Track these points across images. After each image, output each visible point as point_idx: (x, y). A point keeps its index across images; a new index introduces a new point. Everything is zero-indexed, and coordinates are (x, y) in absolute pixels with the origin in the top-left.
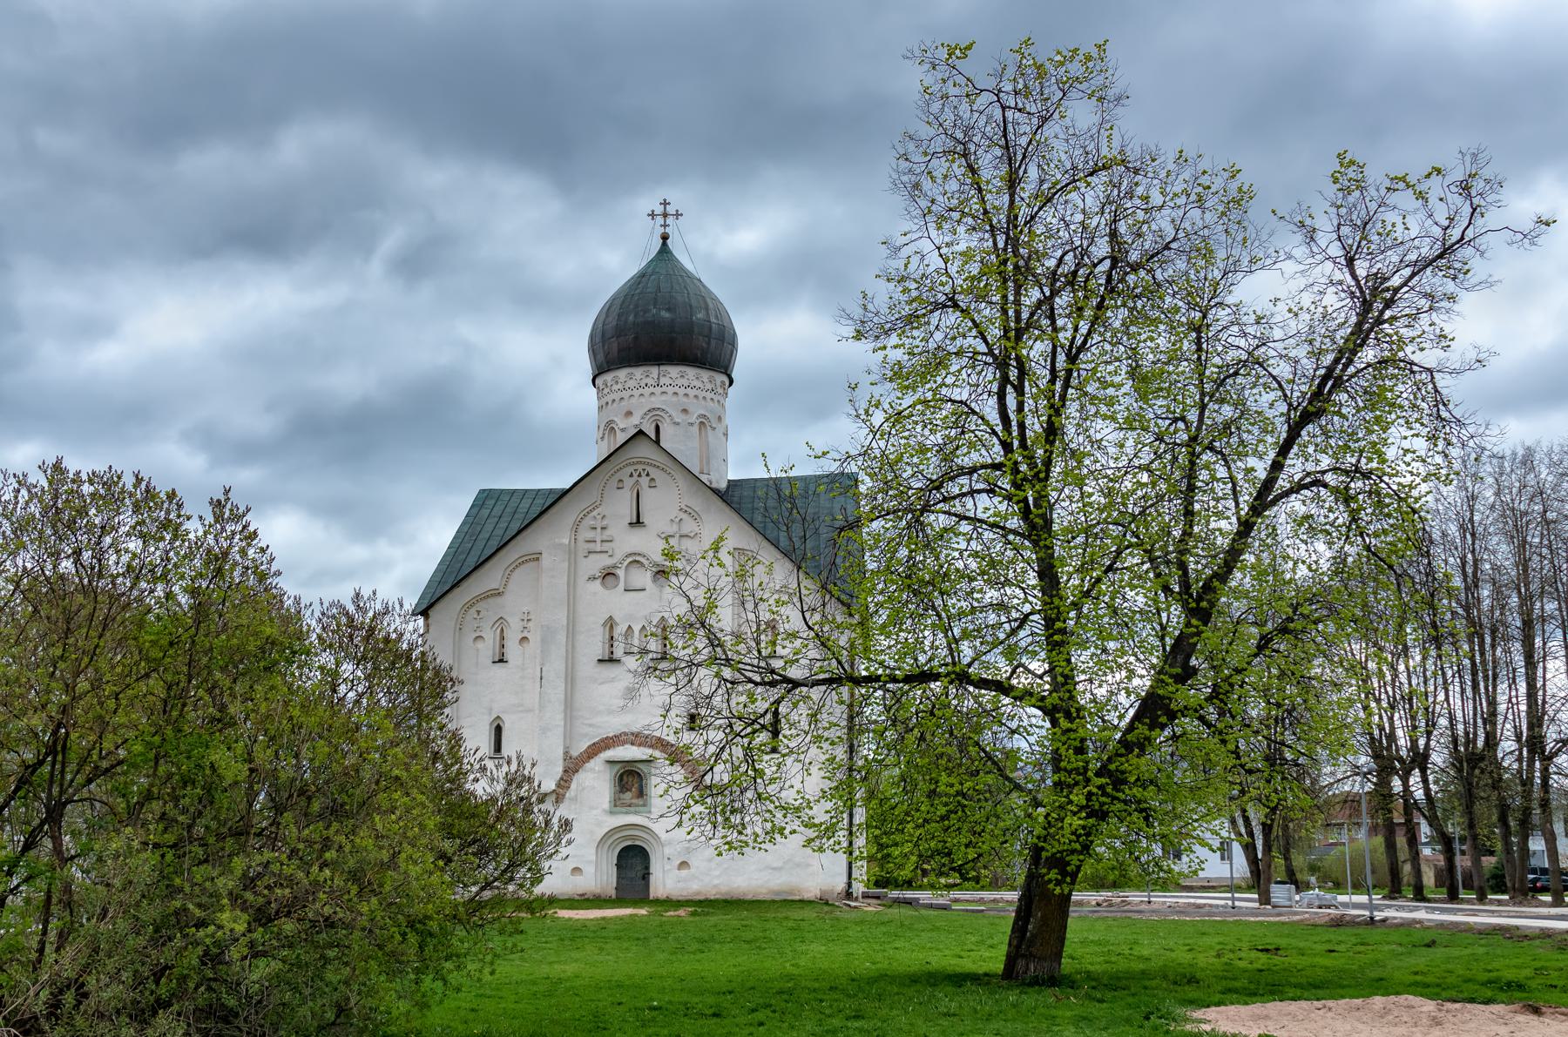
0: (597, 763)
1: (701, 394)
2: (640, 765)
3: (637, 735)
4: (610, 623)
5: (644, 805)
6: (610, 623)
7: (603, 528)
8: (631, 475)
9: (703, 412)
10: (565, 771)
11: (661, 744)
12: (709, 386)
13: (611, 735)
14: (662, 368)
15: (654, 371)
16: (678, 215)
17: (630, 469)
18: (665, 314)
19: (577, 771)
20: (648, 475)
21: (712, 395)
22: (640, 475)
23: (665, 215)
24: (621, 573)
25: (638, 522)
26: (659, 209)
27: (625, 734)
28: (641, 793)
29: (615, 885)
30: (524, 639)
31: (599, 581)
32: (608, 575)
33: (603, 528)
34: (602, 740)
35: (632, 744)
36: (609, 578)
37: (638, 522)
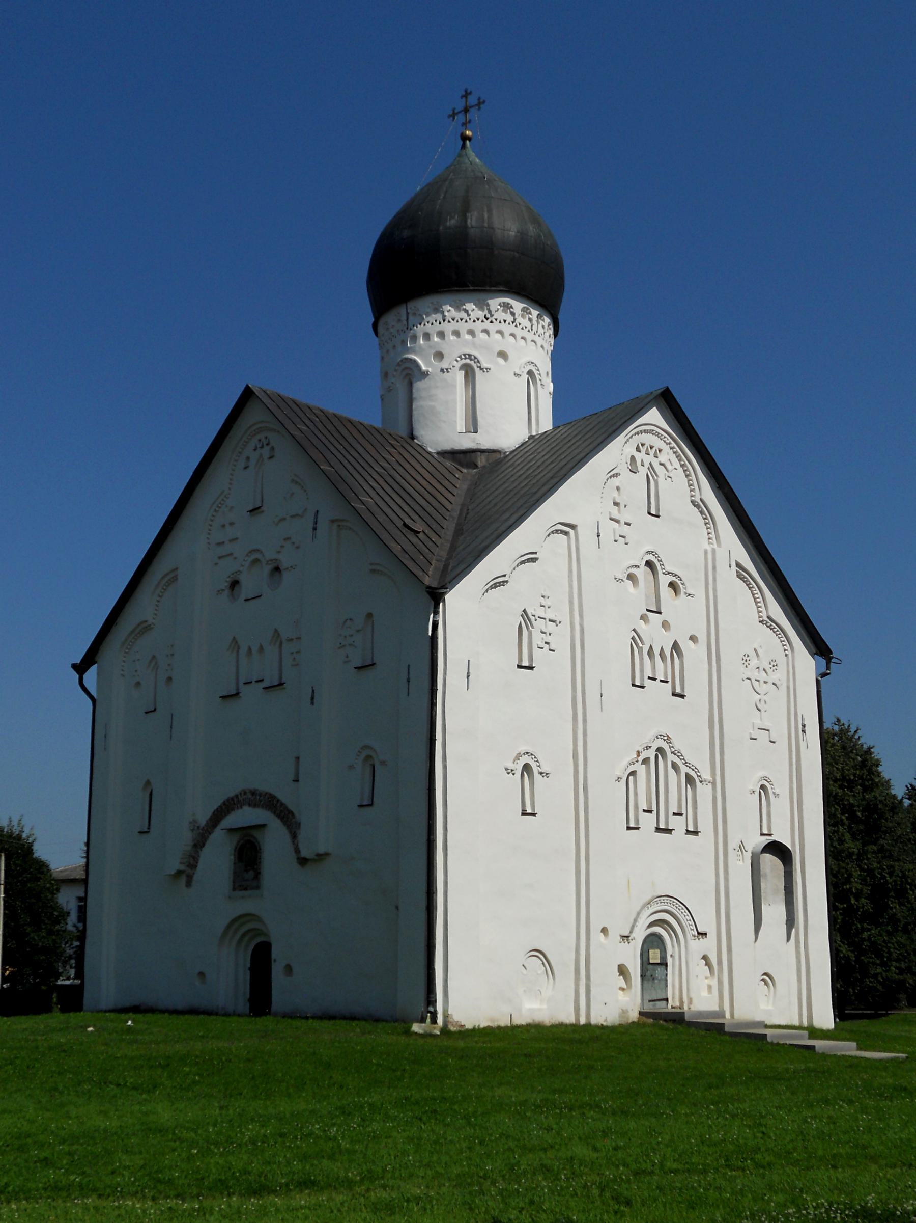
0: (218, 834)
1: (463, 327)
2: (255, 833)
3: (253, 793)
4: (235, 644)
5: (258, 887)
6: (235, 644)
7: (232, 524)
8: (255, 450)
9: (468, 351)
10: (195, 846)
11: (271, 803)
12: (480, 314)
13: (232, 794)
14: (412, 305)
15: (402, 310)
16: (480, 103)
17: (254, 442)
18: (406, 233)
19: (204, 845)
20: (267, 444)
21: (487, 325)
22: (262, 447)
23: (466, 110)
24: (243, 578)
25: (255, 511)
26: (460, 106)
27: (245, 793)
28: (257, 875)
29: (248, 996)
30: (170, 679)
31: (227, 592)
32: (234, 584)
33: (232, 524)
34: (224, 803)
35: (250, 805)
36: (236, 588)
37: (255, 511)
